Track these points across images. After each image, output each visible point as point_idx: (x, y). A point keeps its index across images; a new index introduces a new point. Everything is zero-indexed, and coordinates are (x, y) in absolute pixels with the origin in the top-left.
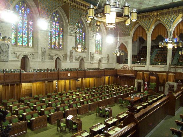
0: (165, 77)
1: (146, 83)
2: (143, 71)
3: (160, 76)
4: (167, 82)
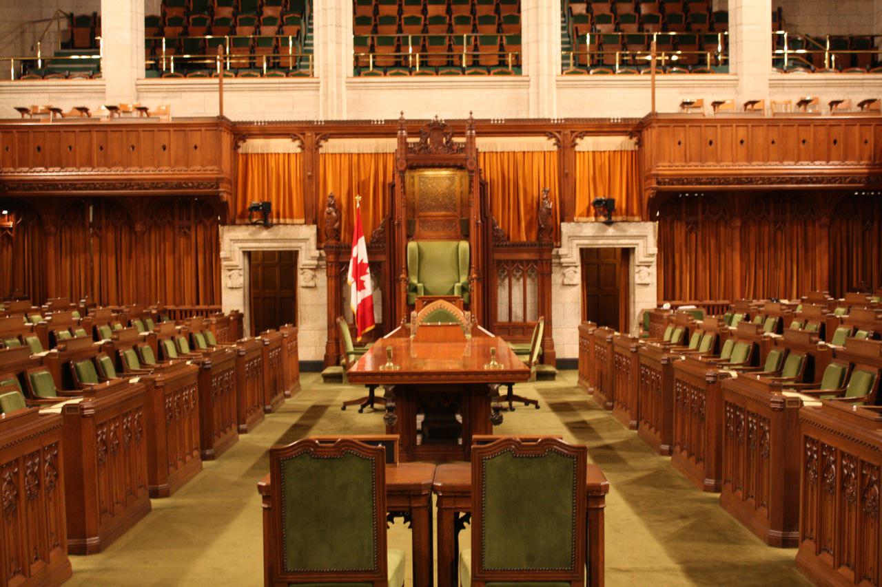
0: (540, 180)
1: (360, 251)
2: (311, 134)
3: (491, 172)
4: (566, 228)
